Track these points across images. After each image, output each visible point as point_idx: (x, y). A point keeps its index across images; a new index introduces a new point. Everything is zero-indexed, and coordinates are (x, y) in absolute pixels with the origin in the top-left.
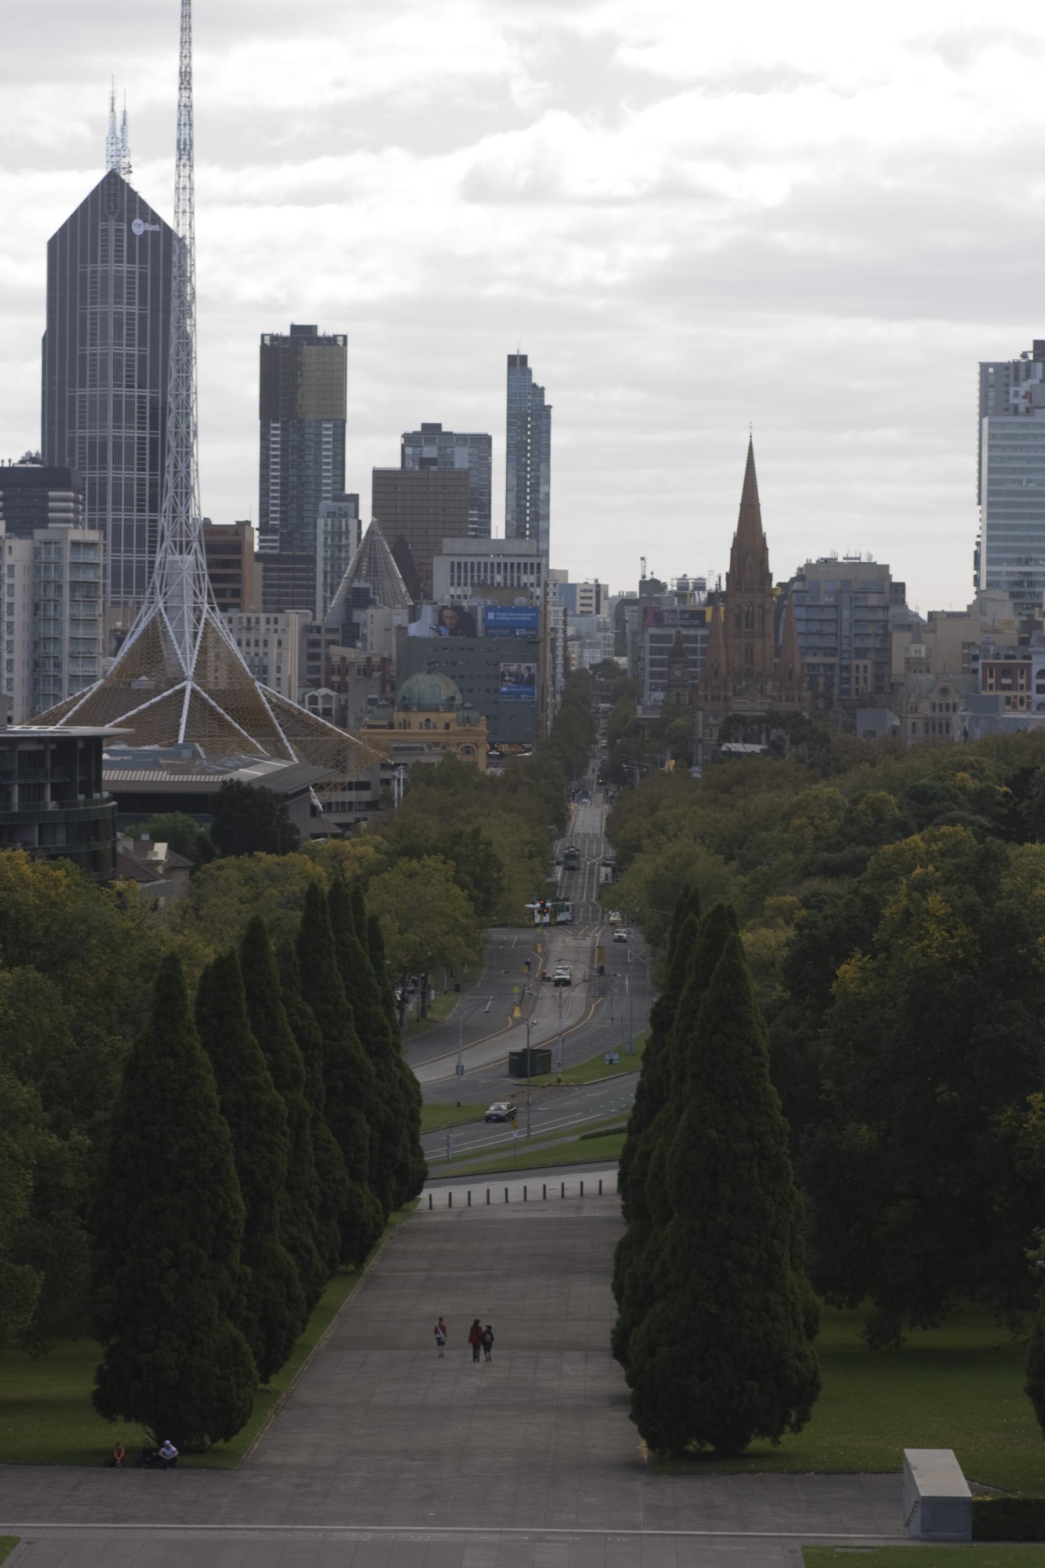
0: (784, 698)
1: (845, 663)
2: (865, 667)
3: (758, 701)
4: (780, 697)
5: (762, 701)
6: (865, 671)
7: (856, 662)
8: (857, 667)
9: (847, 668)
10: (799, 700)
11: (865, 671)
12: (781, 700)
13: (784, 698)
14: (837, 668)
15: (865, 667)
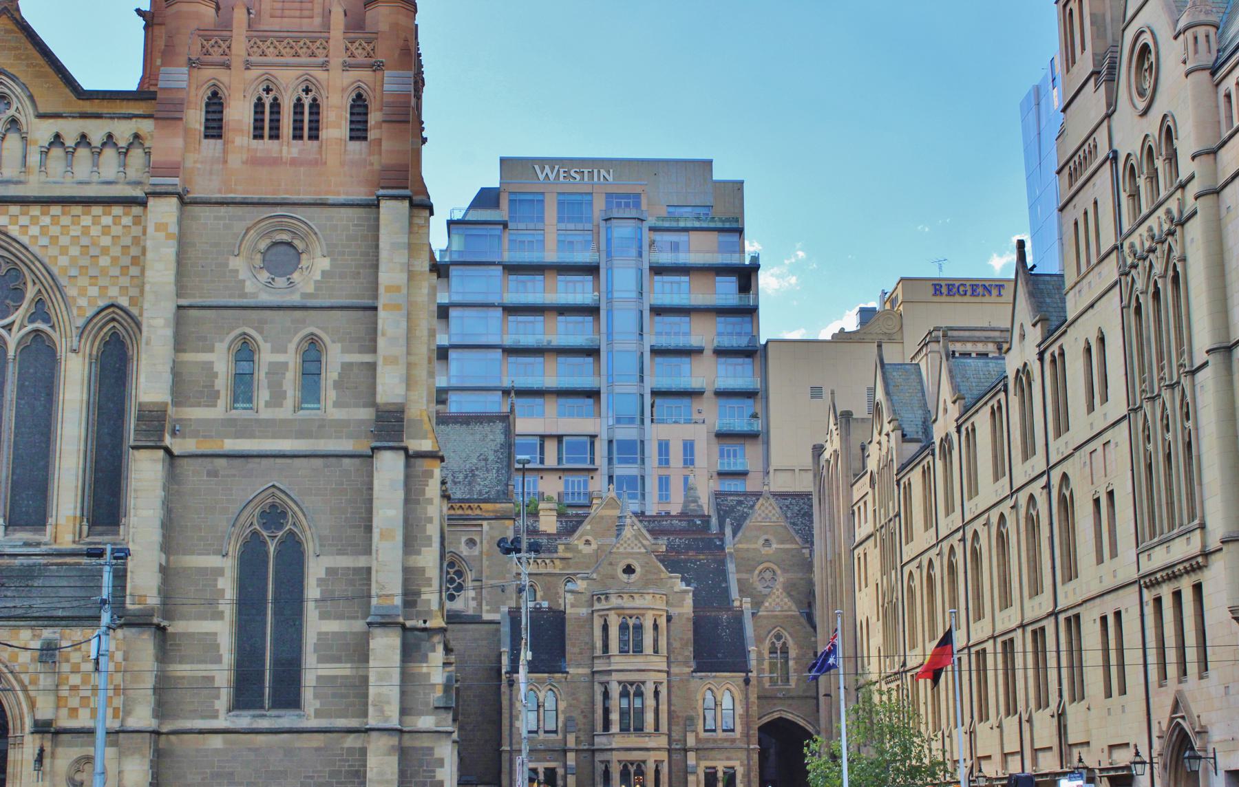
0: (239, 113)
1: (626, 433)
2: (689, 447)
3: (43, 131)
4: (215, 104)
5: (70, 129)
6: (689, 461)
7: (654, 433)
8: (664, 447)
9: (632, 450)
10: (358, 132)
11: (689, 461)
12: (215, 128)
13: (239, 113)
14: (601, 448)
15: (689, 447)
